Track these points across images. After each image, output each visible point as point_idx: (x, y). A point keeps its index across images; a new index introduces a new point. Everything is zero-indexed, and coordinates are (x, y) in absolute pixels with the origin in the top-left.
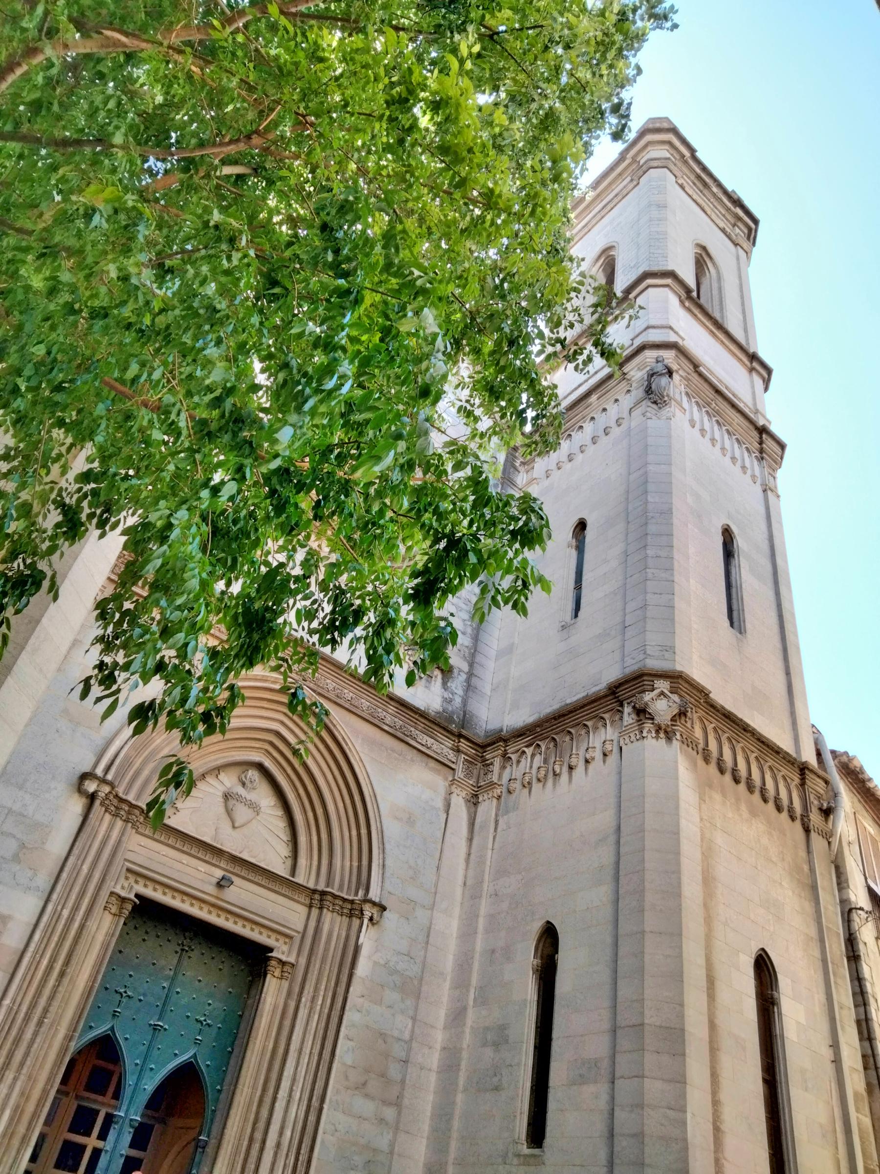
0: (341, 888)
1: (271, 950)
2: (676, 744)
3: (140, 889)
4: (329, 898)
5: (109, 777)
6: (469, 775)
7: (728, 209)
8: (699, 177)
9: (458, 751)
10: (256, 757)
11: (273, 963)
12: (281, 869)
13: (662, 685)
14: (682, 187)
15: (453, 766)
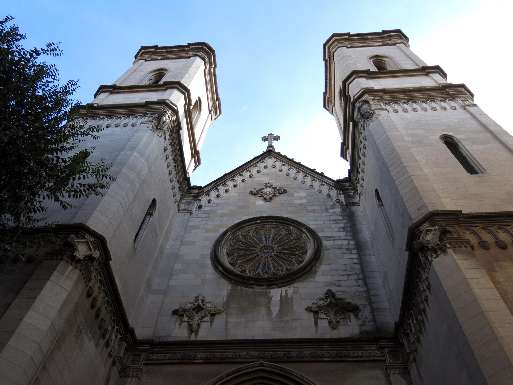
2: (450, 251)
7: (382, 38)
8: (359, 39)
9: (381, 349)
13: (425, 226)
14: (352, 47)
15: (383, 359)
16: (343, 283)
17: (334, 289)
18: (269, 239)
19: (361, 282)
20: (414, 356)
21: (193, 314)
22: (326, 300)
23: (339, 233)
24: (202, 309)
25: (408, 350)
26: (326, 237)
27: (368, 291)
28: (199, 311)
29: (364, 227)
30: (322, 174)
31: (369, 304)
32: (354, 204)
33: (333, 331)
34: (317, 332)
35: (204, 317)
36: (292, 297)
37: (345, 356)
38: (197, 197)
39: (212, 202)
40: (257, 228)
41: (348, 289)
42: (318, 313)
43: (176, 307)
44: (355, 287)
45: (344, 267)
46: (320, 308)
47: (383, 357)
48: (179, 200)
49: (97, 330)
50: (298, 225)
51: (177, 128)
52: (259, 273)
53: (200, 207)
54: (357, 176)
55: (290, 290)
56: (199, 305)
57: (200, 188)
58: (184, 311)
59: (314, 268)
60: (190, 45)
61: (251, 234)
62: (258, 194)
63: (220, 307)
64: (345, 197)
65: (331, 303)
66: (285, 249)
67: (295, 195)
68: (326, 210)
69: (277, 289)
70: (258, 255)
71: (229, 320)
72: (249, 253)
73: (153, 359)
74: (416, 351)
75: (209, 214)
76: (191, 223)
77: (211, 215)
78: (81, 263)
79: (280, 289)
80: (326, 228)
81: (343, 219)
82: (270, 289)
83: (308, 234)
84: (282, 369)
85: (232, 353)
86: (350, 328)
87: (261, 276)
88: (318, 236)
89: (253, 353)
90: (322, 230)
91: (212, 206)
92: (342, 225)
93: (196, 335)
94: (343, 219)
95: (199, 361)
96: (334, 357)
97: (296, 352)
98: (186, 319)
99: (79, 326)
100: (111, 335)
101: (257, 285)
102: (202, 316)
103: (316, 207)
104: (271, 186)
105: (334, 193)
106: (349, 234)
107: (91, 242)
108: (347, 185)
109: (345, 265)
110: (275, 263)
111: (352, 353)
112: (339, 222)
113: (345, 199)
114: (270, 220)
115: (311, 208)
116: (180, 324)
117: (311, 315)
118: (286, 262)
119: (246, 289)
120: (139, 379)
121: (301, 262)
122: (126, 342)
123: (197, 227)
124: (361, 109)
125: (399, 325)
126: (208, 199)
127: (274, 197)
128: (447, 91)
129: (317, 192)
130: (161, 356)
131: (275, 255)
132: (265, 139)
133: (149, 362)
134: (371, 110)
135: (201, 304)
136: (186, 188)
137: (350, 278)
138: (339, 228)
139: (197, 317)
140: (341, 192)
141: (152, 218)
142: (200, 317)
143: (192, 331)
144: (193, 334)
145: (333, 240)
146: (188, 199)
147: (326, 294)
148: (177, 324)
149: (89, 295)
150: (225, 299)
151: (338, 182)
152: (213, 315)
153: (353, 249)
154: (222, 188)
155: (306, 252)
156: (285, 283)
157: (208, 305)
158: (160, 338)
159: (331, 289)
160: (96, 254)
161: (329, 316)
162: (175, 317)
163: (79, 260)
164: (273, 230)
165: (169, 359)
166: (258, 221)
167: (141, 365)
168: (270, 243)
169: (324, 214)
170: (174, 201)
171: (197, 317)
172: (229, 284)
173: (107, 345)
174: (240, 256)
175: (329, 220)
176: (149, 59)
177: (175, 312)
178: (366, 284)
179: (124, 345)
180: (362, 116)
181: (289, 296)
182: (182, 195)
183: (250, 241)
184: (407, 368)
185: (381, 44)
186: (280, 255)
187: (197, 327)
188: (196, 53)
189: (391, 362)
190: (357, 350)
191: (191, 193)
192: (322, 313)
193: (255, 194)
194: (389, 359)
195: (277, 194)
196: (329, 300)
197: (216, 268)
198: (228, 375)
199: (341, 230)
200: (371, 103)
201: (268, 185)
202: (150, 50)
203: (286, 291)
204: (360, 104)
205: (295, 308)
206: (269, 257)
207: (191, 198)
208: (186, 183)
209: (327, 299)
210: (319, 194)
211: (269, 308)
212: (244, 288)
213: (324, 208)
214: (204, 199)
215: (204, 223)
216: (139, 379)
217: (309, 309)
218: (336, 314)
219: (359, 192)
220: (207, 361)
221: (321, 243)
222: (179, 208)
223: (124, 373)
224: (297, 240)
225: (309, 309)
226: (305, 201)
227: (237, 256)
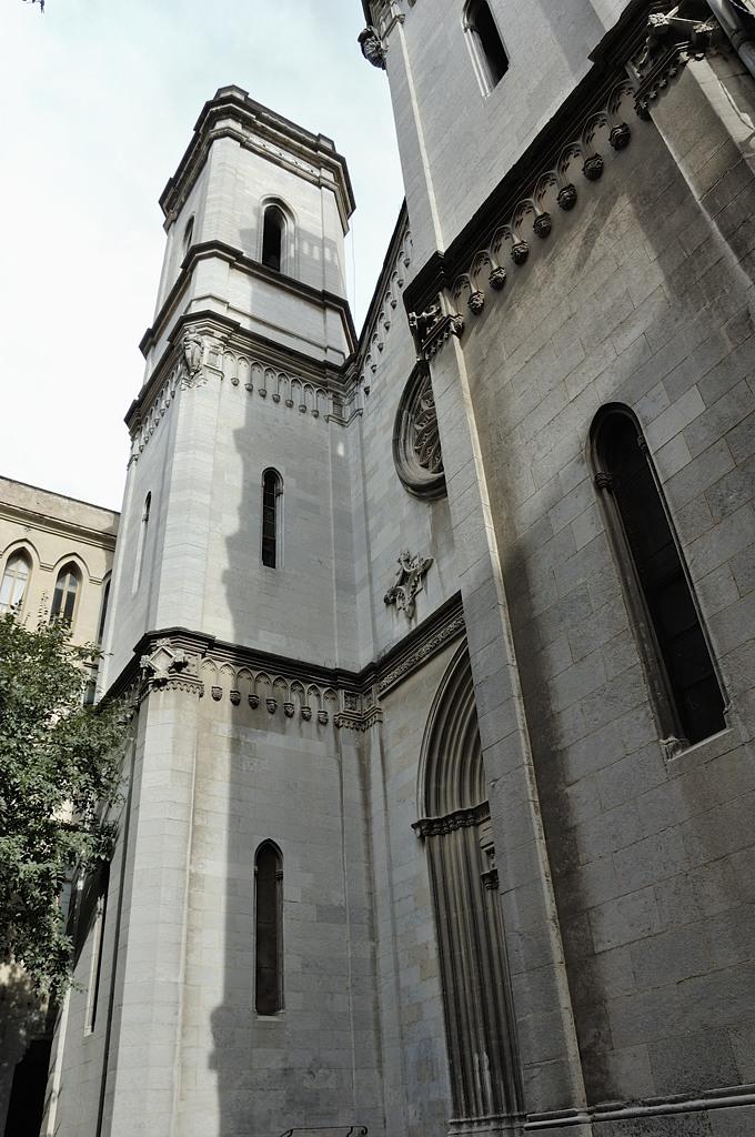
5: (425, 817)
35: (416, 586)
38: (358, 378)
49: (270, 716)
51: (229, 329)
60: (197, 129)
95: (424, 659)
144: (413, 621)
152: (424, 575)
179: (341, 694)
187: (411, 608)
188: (206, 140)
202: (170, 195)
208: (329, 372)
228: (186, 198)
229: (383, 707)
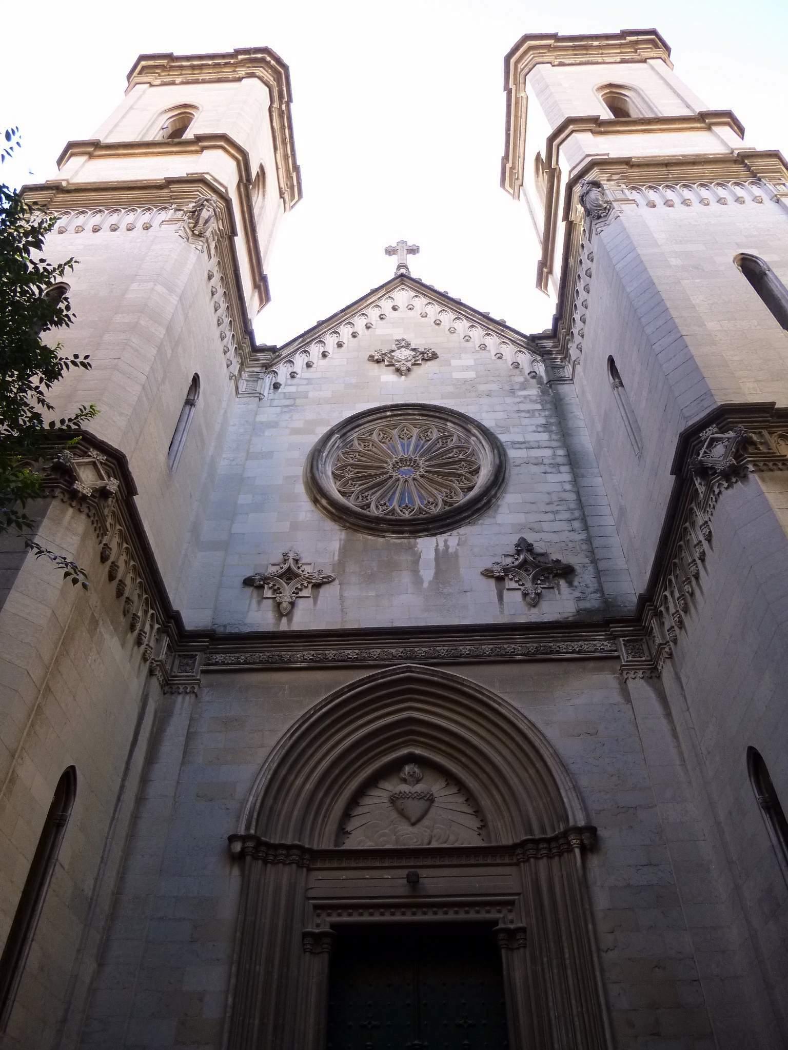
0: (543, 830)
1: (496, 922)
3: (335, 919)
4: (530, 846)
6: (638, 652)
7: (620, 46)
8: (574, 48)
9: (613, 637)
10: (405, 751)
11: (501, 936)
12: (476, 841)
14: (562, 64)
15: (616, 654)
16: (546, 526)
17: (530, 538)
18: (409, 445)
19: (577, 525)
20: (670, 649)
21: (280, 584)
22: (516, 557)
23: (537, 434)
24: (297, 576)
25: (658, 641)
26: (513, 443)
27: (589, 540)
28: (290, 579)
29: (581, 424)
30: (501, 324)
31: (592, 562)
32: (561, 380)
33: (529, 609)
34: (502, 612)
35: (301, 590)
36: (456, 554)
37: (552, 652)
38: (268, 367)
39: (298, 376)
40: (386, 426)
41: (556, 538)
42: (504, 579)
43: (249, 573)
44: (567, 534)
45: (546, 498)
46: (506, 570)
47: (615, 651)
48: (236, 373)
49: (122, 619)
50: (462, 420)
51: (228, 231)
52: (394, 509)
53: (276, 386)
54: (570, 328)
55: (451, 540)
56: (289, 569)
57: (273, 349)
58: (266, 579)
59: (494, 500)
60: (238, 52)
61: (375, 437)
62: (383, 361)
63: (328, 572)
64: (546, 367)
65: (525, 561)
66: (439, 466)
67: (454, 362)
68: (512, 392)
69: (428, 538)
70: (398, 480)
71: (345, 594)
72: (375, 472)
73: (217, 664)
74: (675, 641)
75: (295, 399)
76: (261, 418)
77: (298, 401)
78: (88, 503)
79: (434, 538)
80: (514, 426)
81: (543, 409)
82: (415, 538)
83: (481, 437)
84: (445, 676)
85: (357, 651)
86: (560, 604)
87: (399, 514)
88: (499, 441)
89: (394, 651)
90: (506, 430)
91: (298, 385)
92: (542, 421)
93: (290, 621)
94: (543, 409)
95: (298, 665)
96: (533, 654)
97: (468, 647)
98: (268, 593)
99: (93, 614)
100: (144, 625)
101: (393, 532)
102: (297, 588)
103: (494, 387)
104: (407, 345)
105: (525, 359)
106: (554, 437)
107: (101, 463)
108: (549, 344)
109: (549, 493)
110: (423, 492)
111: (562, 646)
112: (537, 414)
113: (547, 371)
114: (410, 412)
115: (482, 388)
116: (259, 603)
117: (492, 583)
118: (443, 490)
119: (373, 538)
120: (196, 696)
121: (470, 489)
122: (168, 635)
123: (274, 425)
124: (587, 199)
125: (647, 599)
126: (291, 370)
127: (415, 367)
128: (746, 165)
129: (494, 358)
130: (230, 658)
131: (421, 476)
132: (390, 251)
133: (212, 668)
134: (607, 202)
135: (293, 566)
136: (248, 349)
137: (559, 517)
138: (537, 426)
139: (287, 591)
140: (539, 358)
141: (193, 409)
142: (294, 590)
143: (281, 615)
144: (284, 620)
145: (527, 448)
146: (253, 372)
147: (517, 545)
148: (254, 601)
149: (104, 558)
150: (336, 558)
151: (534, 339)
152: (317, 586)
153: (563, 465)
154: (315, 350)
155: (477, 471)
156: (443, 526)
157: (308, 569)
158: (225, 626)
159: (525, 536)
160: (113, 485)
161: (523, 585)
162: (249, 590)
163: (85, 497)
164: (415, 431)
165: (246, 663)
166: (388, 414)
167: (197, 673)
168: (410, 453)
169: (509, 400)
170: (228, 375)
171: (287, 591)
172: (341, 530)
173: (139, 642)
174: (359, 479)
175: (519, 411)
176: (158, 82)
177: (248, 582)
178: (586, 528)
179: (166, 641)
180: (588, 213)
181: (450, 550)
182: (242, 364)
183: (374, 449)
184: (656, 668)
185: (618, 59)
186: (430, 476)
187: (289, 607)
189: (630, 659)
190: (572, 641)
191: (258, 360)
192: (511, 579)
193: (378, 362)
194: (625, 657)
195: (420, 362)
196: (522, 558)
197: (315, 501)
198: (352, 687)
199: (540, 429)
200: (605, 186)
201: (403, 344)
203: (446, 541)
204: (585, 188)
205: (462, 571)
206: (410, 480)
207: (258, 369)
208: (248, 341)
209: (519, 555)
210: (499, 361)
211: (415, 572)
212: (370, 537)
213: (507, 388)
214: (283, 370)
215: (286, 417)
216: (196, 696)
217: (488, 574)
218: (535, 579)
219: (573, 358)
220: (312, 665)
221: (505, 454)
222: (237, 388)
223: (169, 686)
224: (461, 449)
225: (488, 574)
226: (471, 375)
227: (352, 479)
228: (182, 83)
229: (203, 682)
